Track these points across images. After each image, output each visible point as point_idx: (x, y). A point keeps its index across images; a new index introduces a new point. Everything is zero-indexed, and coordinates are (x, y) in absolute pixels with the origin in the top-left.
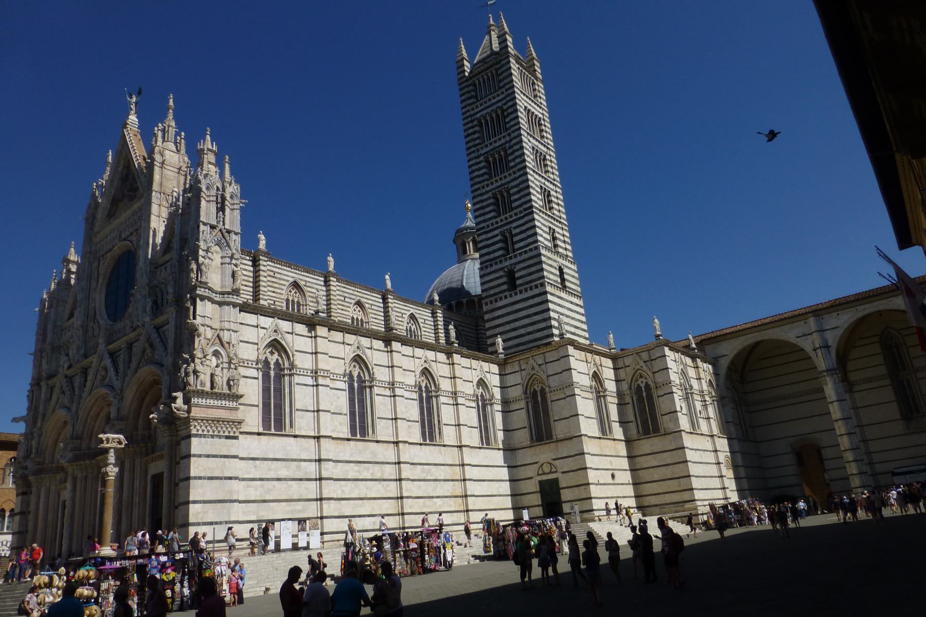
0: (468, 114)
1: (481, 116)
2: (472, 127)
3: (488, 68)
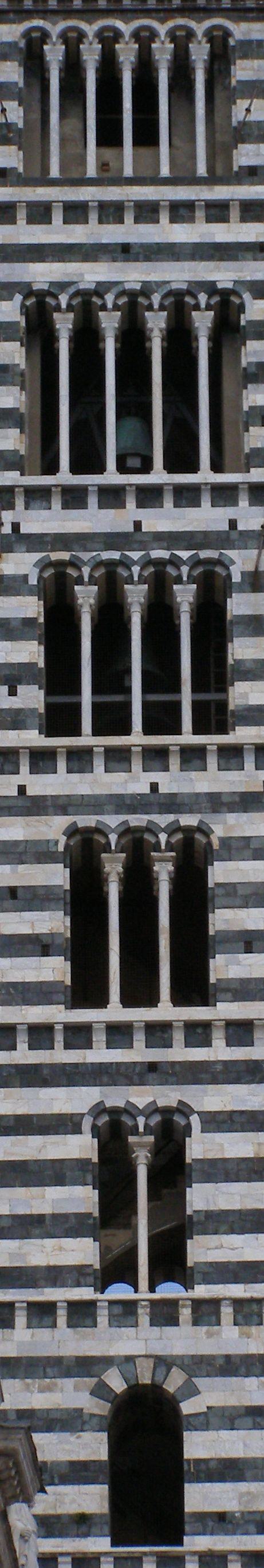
1: (63, 286)
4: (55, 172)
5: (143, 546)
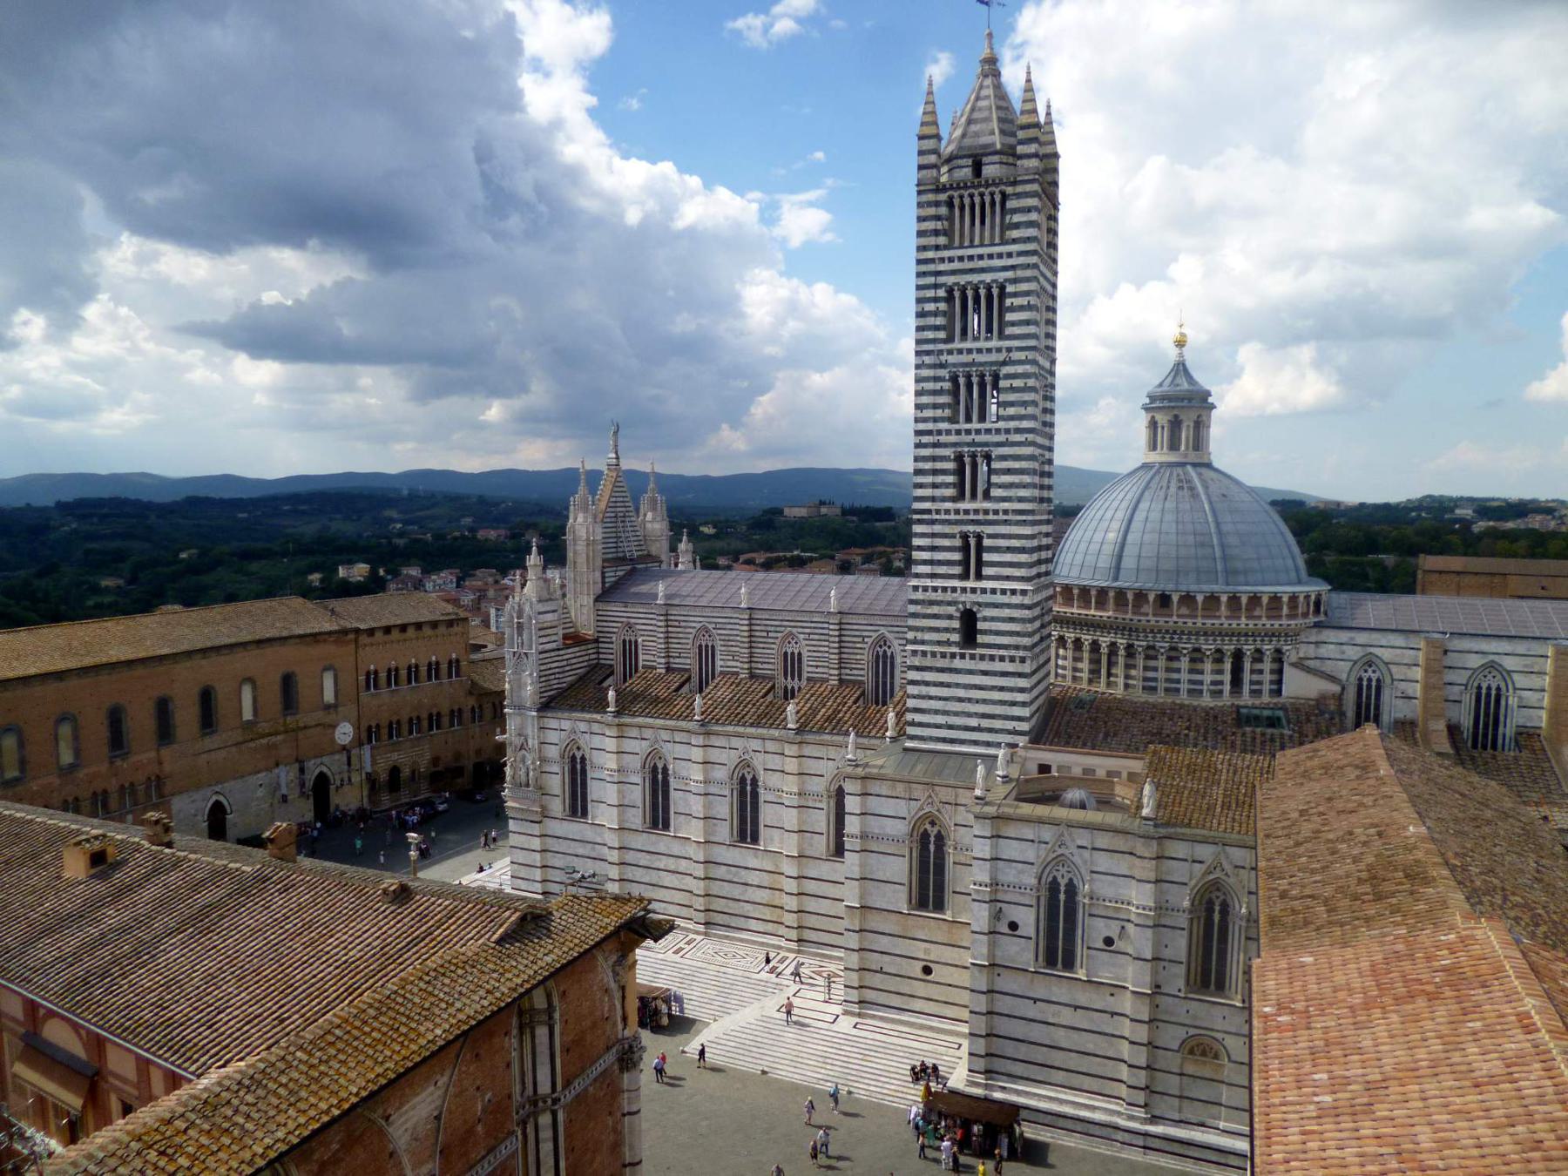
0: (931, 267)
2: (936, 300)
3: (987, 185)
4: (957, 243)
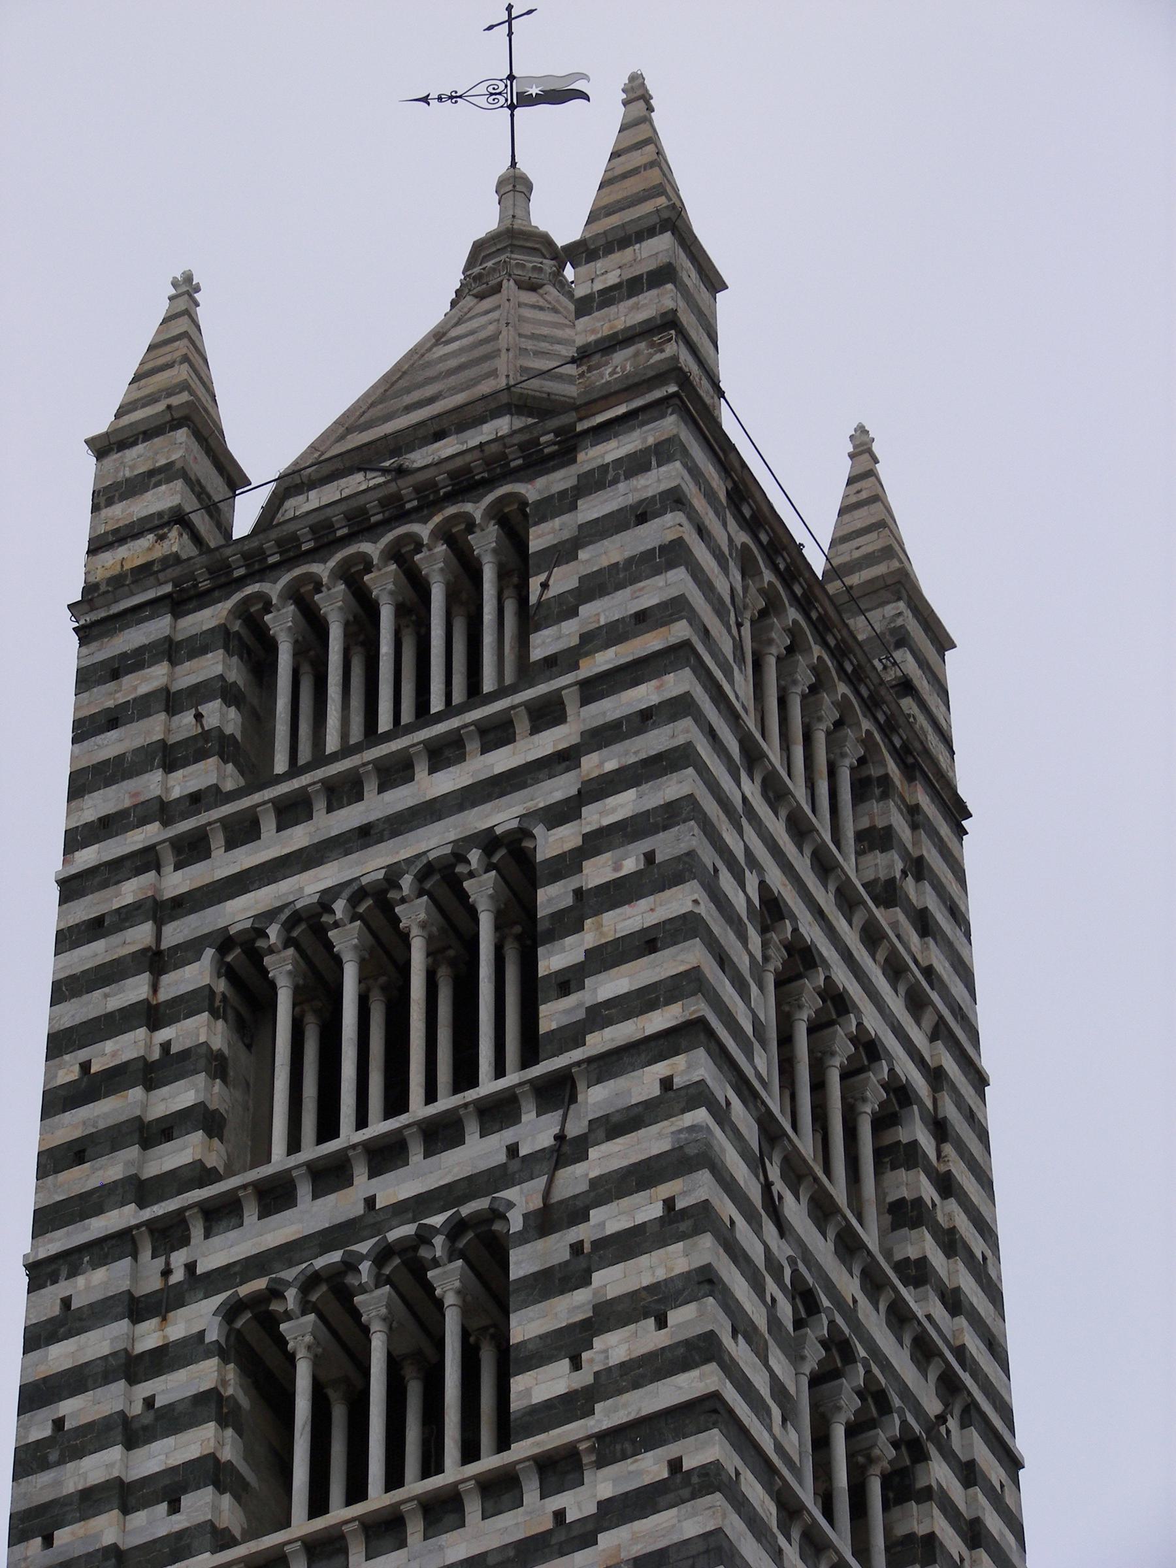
0: (130, 891)
1: (270, 915)
5: (378, 1229)
